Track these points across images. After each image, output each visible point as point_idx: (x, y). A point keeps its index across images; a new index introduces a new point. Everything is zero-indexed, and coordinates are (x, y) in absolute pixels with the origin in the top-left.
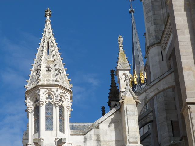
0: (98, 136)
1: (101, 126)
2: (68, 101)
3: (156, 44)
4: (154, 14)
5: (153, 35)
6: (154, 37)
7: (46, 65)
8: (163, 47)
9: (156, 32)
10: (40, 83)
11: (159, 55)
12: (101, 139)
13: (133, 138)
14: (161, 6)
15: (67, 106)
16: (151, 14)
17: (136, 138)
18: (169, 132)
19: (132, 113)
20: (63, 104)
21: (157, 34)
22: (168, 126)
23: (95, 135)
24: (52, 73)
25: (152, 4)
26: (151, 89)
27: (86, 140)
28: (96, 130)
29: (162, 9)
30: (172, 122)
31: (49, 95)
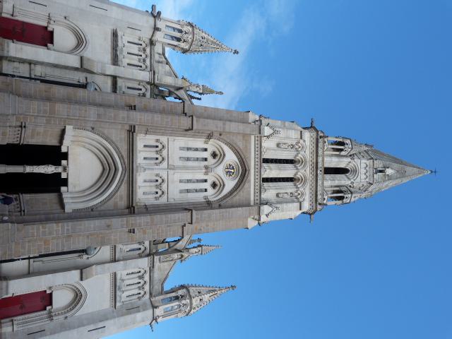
0: (162, 62)
12: (160, 64)
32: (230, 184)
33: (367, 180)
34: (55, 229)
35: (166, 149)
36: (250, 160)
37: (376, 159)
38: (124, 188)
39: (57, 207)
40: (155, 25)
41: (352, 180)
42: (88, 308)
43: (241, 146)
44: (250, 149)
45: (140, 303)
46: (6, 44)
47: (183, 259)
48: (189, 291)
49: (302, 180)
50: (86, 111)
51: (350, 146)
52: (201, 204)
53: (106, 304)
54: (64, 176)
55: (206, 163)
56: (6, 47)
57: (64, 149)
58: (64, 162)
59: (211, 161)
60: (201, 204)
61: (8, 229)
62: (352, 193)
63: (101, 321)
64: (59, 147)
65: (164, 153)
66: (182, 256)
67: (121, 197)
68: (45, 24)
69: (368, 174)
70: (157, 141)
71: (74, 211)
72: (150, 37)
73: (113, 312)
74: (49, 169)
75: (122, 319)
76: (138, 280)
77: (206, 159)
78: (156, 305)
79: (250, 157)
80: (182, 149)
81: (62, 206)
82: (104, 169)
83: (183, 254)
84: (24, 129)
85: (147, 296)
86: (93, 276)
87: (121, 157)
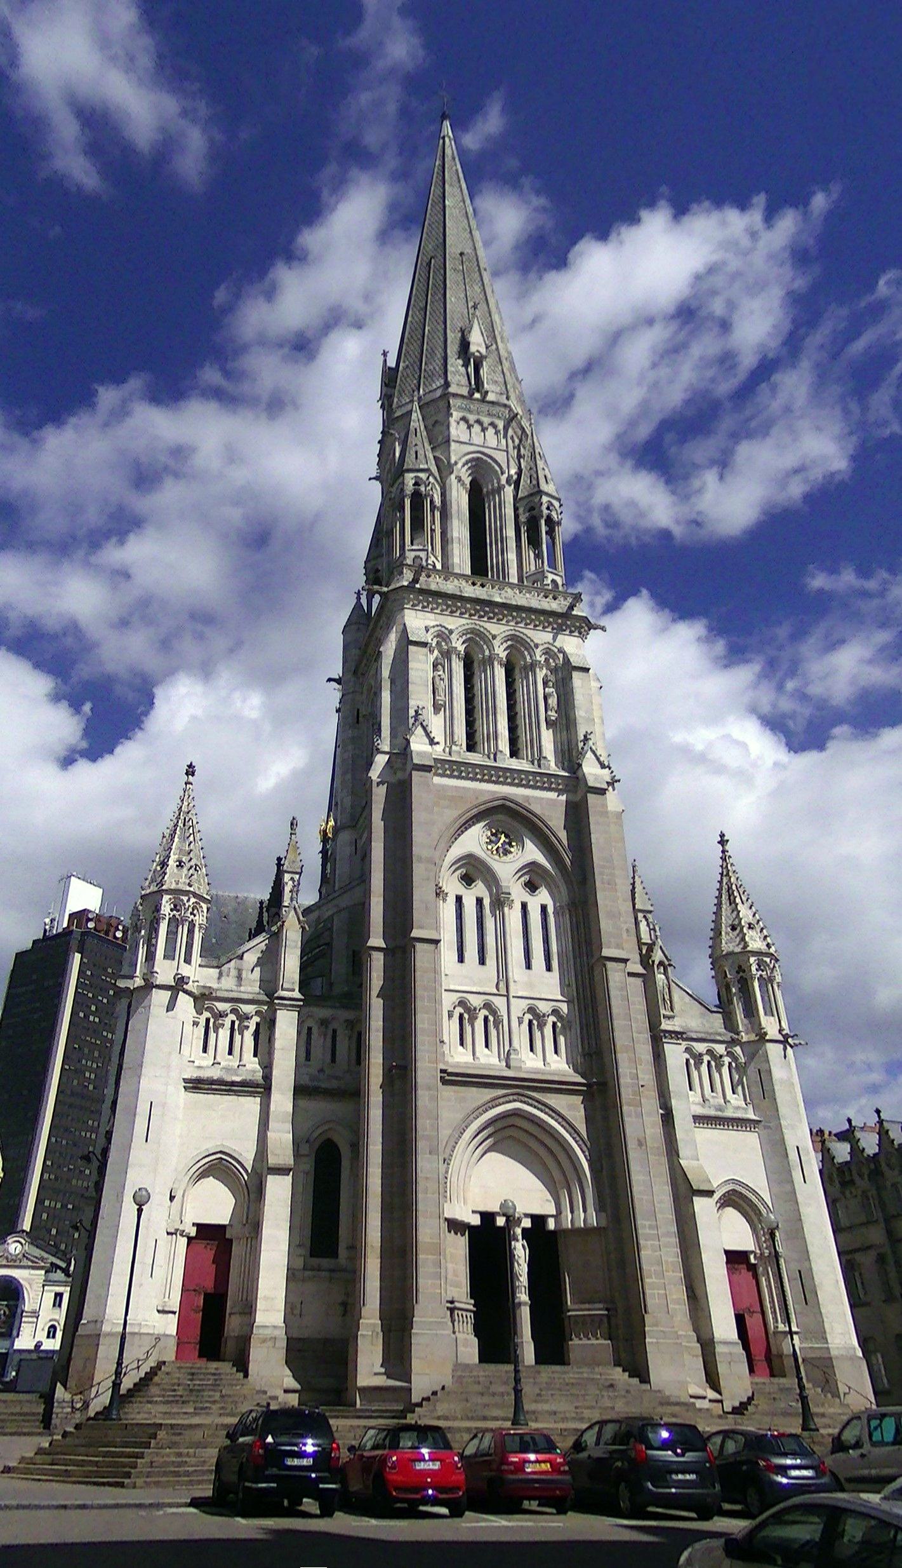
9: (352, 807)
16: (349, 776)
19: (294, 944)
27: (221, 974)
28: (239, 961)
32: (531, 852)
34: (649, 1252)
35: (470, 997)
36: (482, 792)
37: (447, 384)
38: (552, 1100)
42: (757, 1180)
43: (456, 813)
47: (667, 963)
49: (517, 644)
50: (427, 1178)
51: (423, 476)
53: (751, 1139)
54: (527, 1223)
55: (487, 902)
57: (476, 1221)
58: (501, 1221)
61: (657, 1343)
62: (540, 493)
64: (471, 1229)
65: (476, 1001)
66: (661, 963)
67: (571, 1107)
69: (486, 420)
70: (450, 1015)
73: (765, 1127)
74: (520, 1251)
75: (783, 1110)
76: (704, 1068)
79: (475, 790)
80: (461, 959)
83: (656, 963)
84: (457, 1305)
86: (702, 1167)
87: (494, 1103)
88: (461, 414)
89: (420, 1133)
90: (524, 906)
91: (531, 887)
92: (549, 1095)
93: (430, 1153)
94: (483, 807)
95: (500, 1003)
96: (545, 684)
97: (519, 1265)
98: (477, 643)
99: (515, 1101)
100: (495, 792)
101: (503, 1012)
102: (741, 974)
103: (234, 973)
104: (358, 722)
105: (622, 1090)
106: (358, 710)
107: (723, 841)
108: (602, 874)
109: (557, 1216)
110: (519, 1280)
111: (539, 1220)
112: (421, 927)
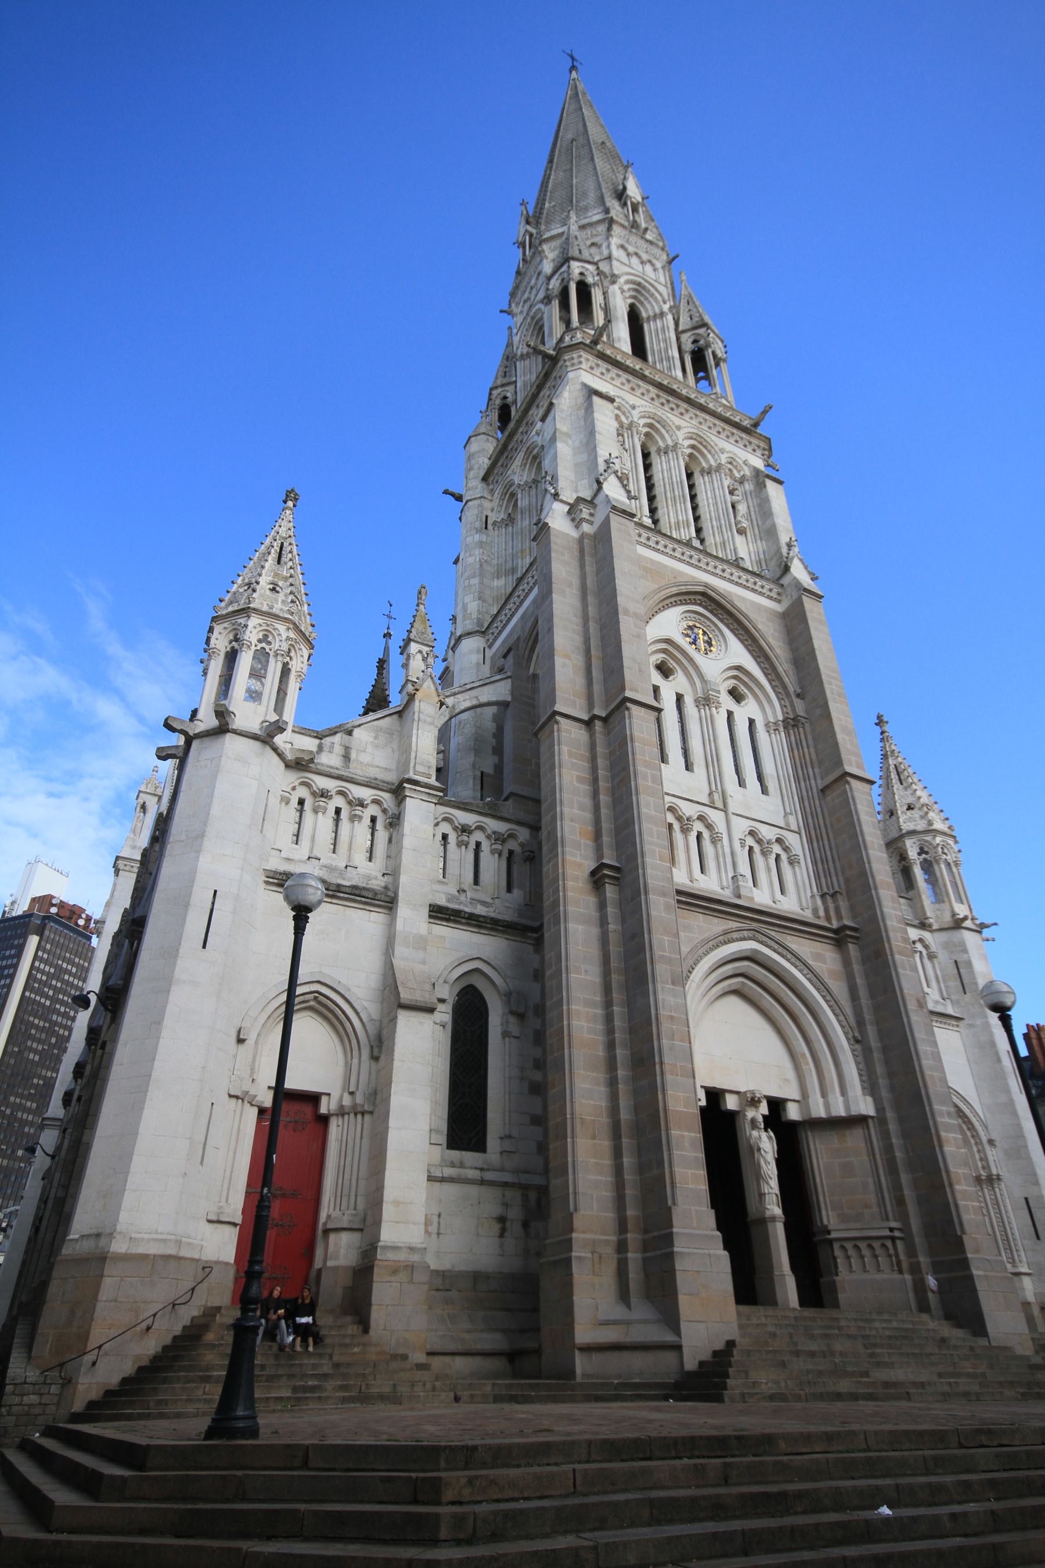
0: (347, 750)
1: (356, 732)
2: (303, 662)
3: (477, 632)
4: (481, 583)
5: (474, 616)
6: (475, 621)
7: (270, 578)
8: (488, 640)
10: (251, 605)
11: (478, 652)
12: (353, 755)
13: (424, 766)
14: (496, 574)
15: (298, 670)
16: (475, 581)
17: (429, 767)
18: (474, 790)
19: (429, 720)
20: (290, 663)
21: (481, 616)
22: (474, 779)
23: (341, 745)
24: (281, 596)
25: (481, 565)
26: (466, 695)
29: (498, 579)
30: (482, 773)
31: (266, 636)
32: (737, 653)
33: (659, 265)
39: (855, 1138)
40: (254, 737)
41: (666, 307)
44: (652, 562)
45: (943, 957)
46: (391, 1256)
48: (912, 833)
50: (672, 1017)
52: (795, 747)
55: (689, 701)
56: (402, 1256)
59: (679, 682)
60: (799, 743)
63: (999, 1060)
65: (688, 810)
67: (818, 957)
68: (251, 1115)
71: (871, 1087)
72: (282, 765)
73: (971, 1026)
77: (679, 698)
78: (947, 918)
79: (673, 570)
81: (861, 1120)
82: (736, 992)
85: (927, 935)
87: (726, 938)
88: (620, 242)
89: (657, 953)
90: (730, 714)
91: (736, 695)
92: (789, 937)
93: (673, 983)
94: (683, 589)
95: (716, 817)
96: (731, 493)
97: (767, 1163)
98: (657, 431)
99: (750, 939)
100: (694, 577)
101: (721, 826)
102: (924, 856)
103: (338, 750)
104: (486, 528)
105: (891, 935)
106: (487, 517)
107: (880, 721)
108: (830, 683)
109: (803, 1101)
110: (768, 1184)
111: (776, 1105)
112: (631, 690)
